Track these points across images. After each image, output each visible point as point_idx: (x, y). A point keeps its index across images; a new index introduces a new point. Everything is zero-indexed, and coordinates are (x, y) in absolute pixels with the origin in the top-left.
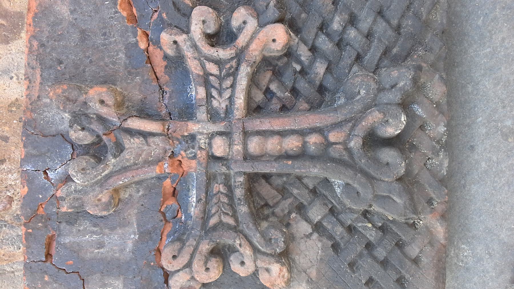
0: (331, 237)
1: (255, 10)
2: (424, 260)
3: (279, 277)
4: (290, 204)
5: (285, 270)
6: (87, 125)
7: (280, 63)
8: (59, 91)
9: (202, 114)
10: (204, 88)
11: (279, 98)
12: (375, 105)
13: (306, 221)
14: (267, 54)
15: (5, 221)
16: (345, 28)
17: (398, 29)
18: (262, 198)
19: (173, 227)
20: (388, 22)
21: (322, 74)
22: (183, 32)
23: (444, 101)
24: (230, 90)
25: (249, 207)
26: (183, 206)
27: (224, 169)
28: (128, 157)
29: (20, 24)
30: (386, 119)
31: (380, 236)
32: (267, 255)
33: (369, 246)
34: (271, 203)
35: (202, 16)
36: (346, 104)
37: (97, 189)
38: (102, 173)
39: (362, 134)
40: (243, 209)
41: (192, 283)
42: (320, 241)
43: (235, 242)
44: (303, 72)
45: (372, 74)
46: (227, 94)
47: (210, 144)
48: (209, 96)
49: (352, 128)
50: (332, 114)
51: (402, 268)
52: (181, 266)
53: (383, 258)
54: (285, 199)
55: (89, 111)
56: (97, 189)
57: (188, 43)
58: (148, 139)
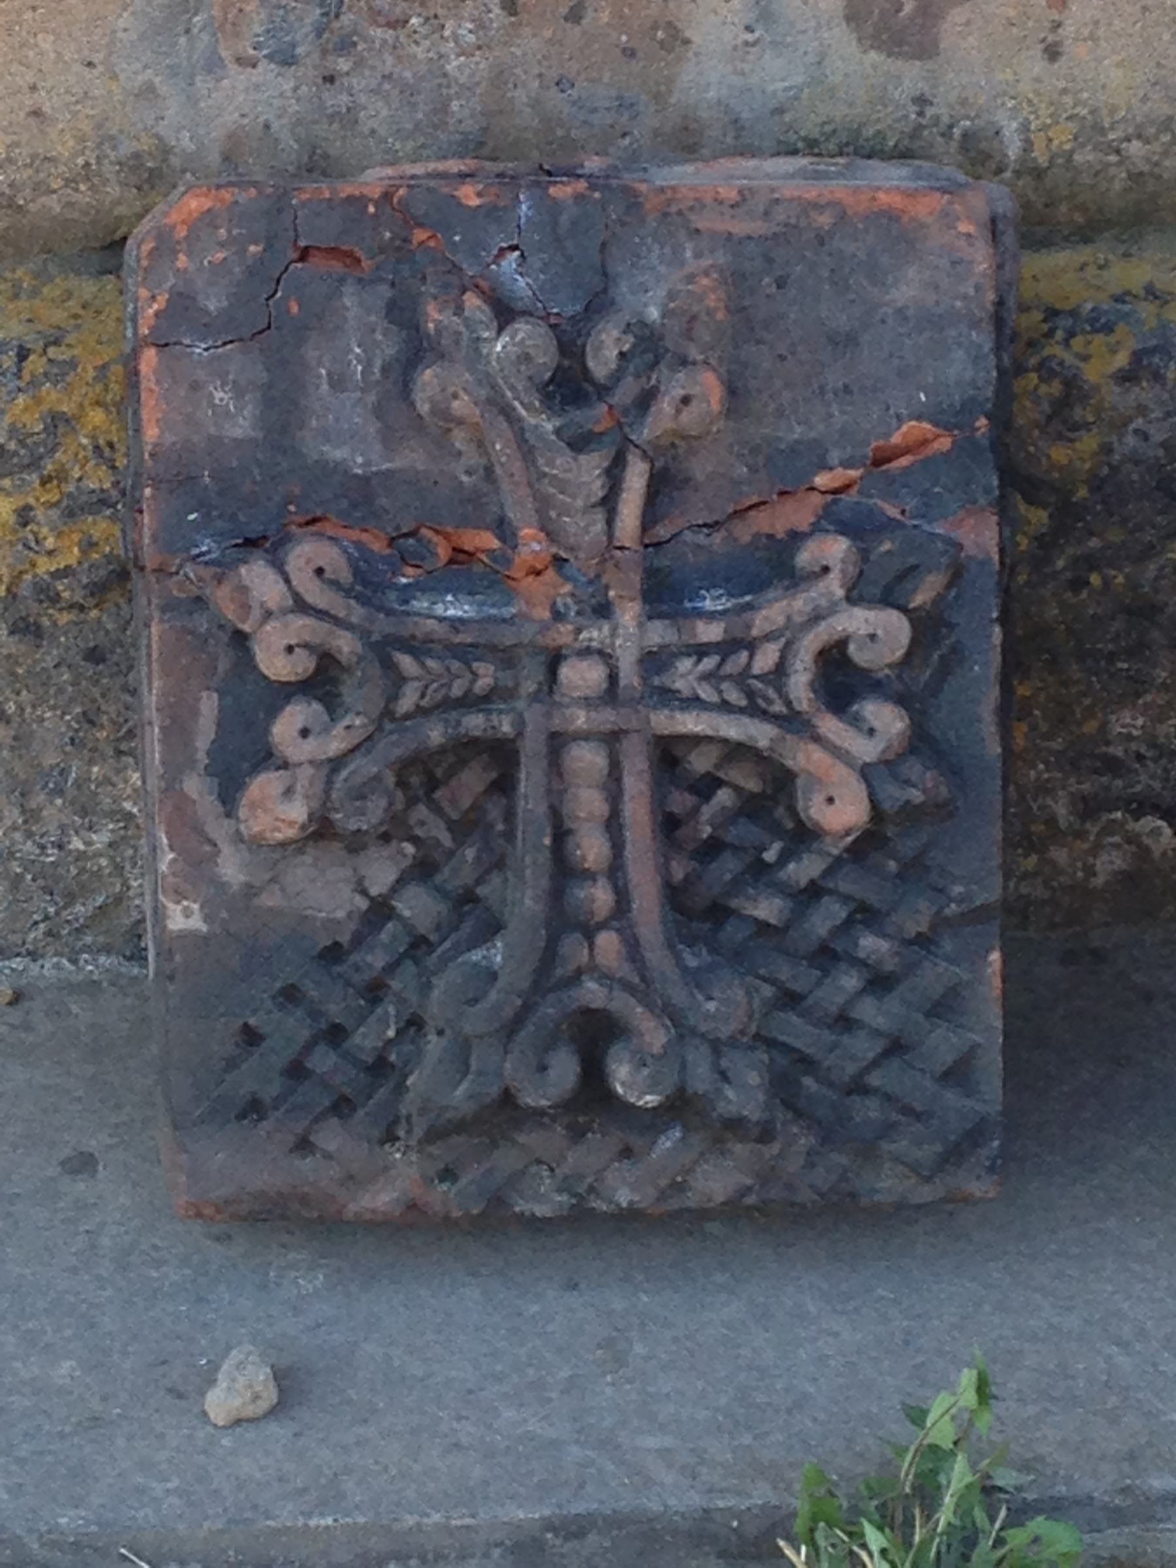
0: (358, 940)
1: (899, 755)
2: (307, 1165)
3: (277, 819)
4: (438, 841)
5: (291, 833)
6: (631, 368)
7: (780, 812)
8: (711, 301)
9: (659, 634)
10: (719, 639)
11: (696, 810)
12: (681, 1037)
13: (398, 881)
14: (800, 782)
15: (337, 16)
16: (863, 964)
17: (858, 1088)
18: (451, 773)
19: (382, 557)
20: (875, 1064)
21: (756, 913)
22: (849, 591)
23: (692, 1200)
24: (714, 698)
25: (442, 750)
26: (433, 585)
27: (529, 687)
28: (558, 462)
29: (906, 48)
30: (649, 1061)
31: (364, 1058)
32: (327, 792)
33: (335, 1035)
34: (438, 795)
35: (887, 632)
36: (685, 970)
37: (483, 392)
38: (522, 403)
39: (614, 1006)
40: (436, 735)
41: (256, 613)
42: (350, 915)
43: (358, 714)
44: (759, 871)
45: (753, 1028)
46: (706, 693)
47: (586, 652)
48: (701, 651)
49: (628, 987)
50: (661, 937)
51: (287, 1111)
52: (301, 590)
53: (309, 1065)
54: (449, 829)
55: (665, 371)
56: (483, 392)
57: (823, 602)
58: (599, 509)
